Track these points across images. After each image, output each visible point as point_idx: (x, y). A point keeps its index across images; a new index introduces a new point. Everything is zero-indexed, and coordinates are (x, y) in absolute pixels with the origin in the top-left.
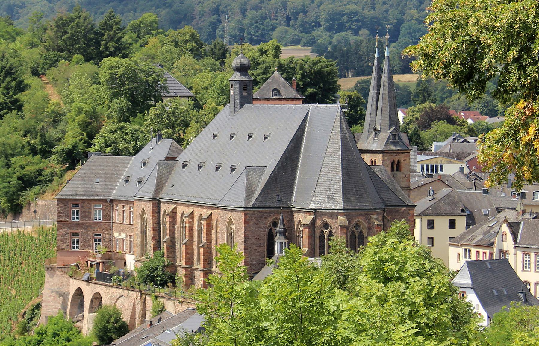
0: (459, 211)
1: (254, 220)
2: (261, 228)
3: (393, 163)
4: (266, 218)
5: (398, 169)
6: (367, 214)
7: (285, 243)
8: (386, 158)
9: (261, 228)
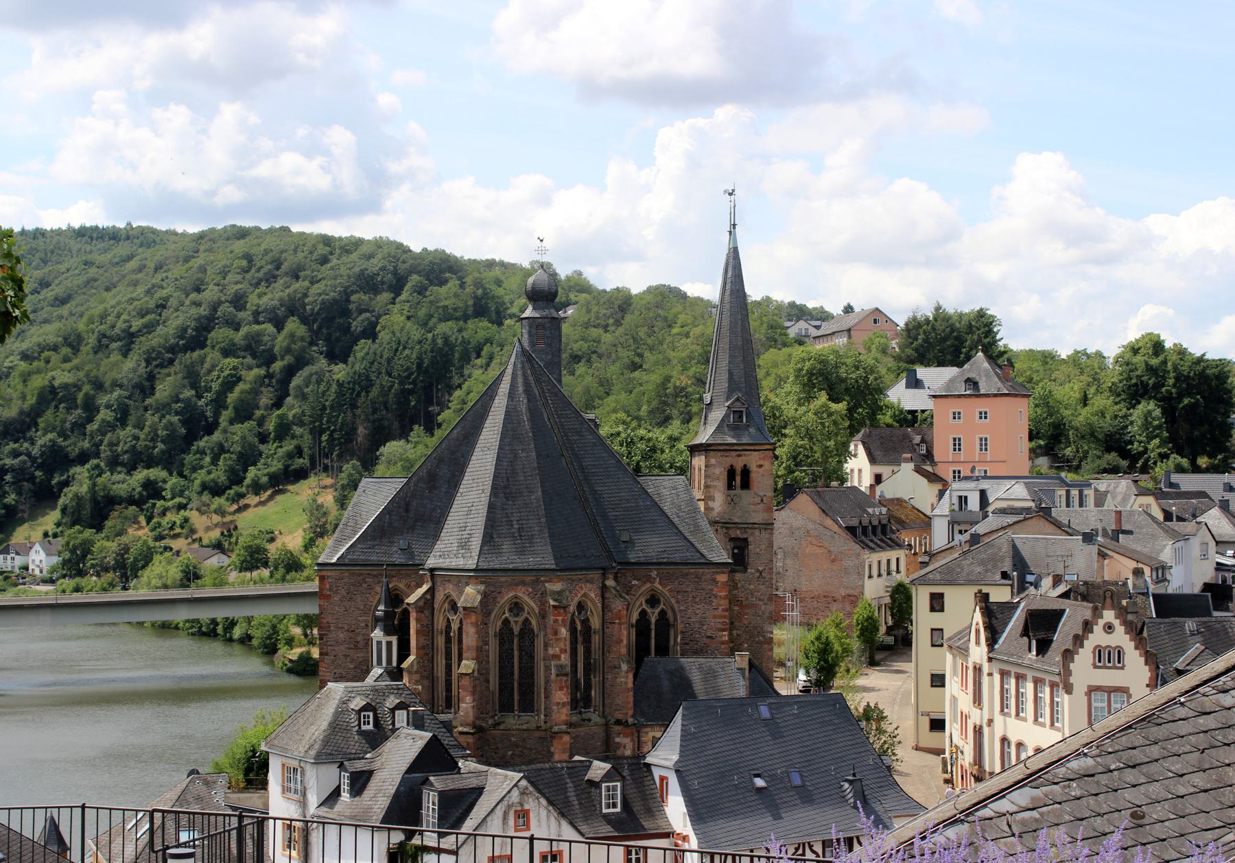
0: (998, 576)
1: (343, 592)
2: (359, 609)
3: (731, 473)
4: (370, 588)
5: (746, 485)
6: (537, 581)
7: (389, 644)
8: (713, 461)
9: (359, 609)
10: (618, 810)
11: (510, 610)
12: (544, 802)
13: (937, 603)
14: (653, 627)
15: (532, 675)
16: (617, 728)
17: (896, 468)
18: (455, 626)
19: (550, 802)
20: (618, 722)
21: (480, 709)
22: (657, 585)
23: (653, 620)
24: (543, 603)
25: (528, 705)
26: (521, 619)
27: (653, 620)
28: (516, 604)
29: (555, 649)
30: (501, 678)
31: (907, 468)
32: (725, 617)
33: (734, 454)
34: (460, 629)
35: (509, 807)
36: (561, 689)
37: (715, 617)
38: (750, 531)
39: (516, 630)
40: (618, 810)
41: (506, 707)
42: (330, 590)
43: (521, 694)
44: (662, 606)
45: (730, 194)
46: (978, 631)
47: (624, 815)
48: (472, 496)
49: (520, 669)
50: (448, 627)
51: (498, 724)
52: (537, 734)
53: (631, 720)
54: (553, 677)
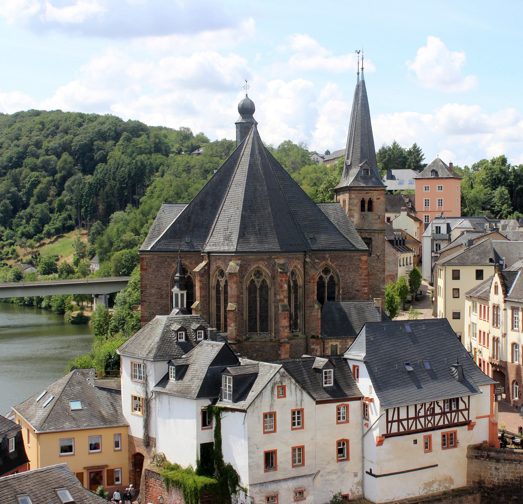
0: (488, 261)
1: (154, 266)
2: (163, 276)
3: (363, 202)
4: (169, 264)
5: (370, 209)
6: (270, 258)
7: (182, 295)
8: (353, 196)
9: (163, 276)
10: (332, 385)
11: (255, 275)
12: (293, 381)
13: (456, 276)
14: (326, 285)
15: (267, 311)
16: (314, 340)
17: (397, 215)
18: (222, 284)
19: (297, 381)
20: (313, 337)
21: (239, 330)
22: (329, 262)
23: (326, 282)
24: (273, 271)
25: (265, 328)
26: (261, 280)
27: (326, 282)
28: (258, 271)
29: (280, 296)
30: (249, 312)
31: (404, 214)
32: (366, 279)
33: (365, 192)
34: (226, 286)
35: (275, 384)
36: (285, 318)
37: (360, 279)
38: (373, 234)
39: (258, 285)
40: (332, 385)
41: (252, 329)
42: (146, 266)
43: (262, 322)
44: (331, 274)
45: (358, 53)
46: (496, 287)
47: (335, 388)
48: (231, 211)
49: (260, 308)
50: (218, 285)
51: (249, 339)
52: (270, 344)
53: (320, 336)
54: (280, 311)
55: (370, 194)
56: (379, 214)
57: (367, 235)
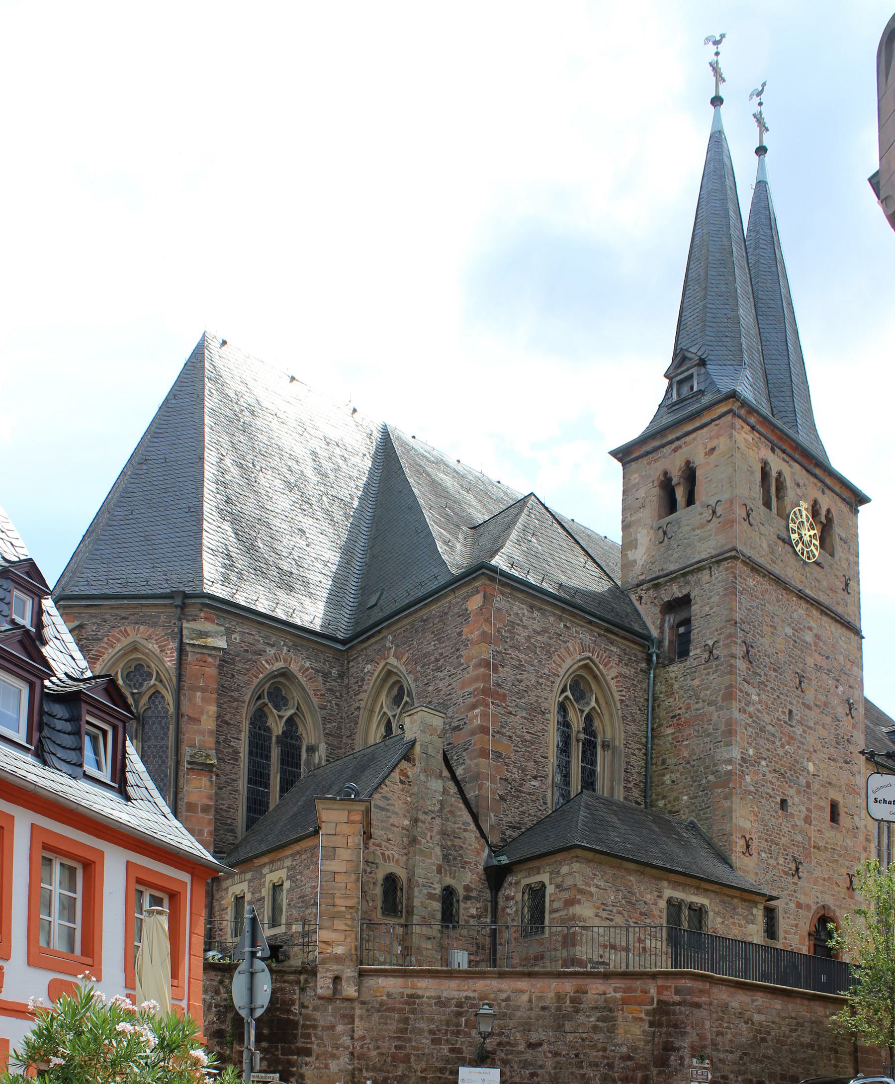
3: (667, 486)
33: (667, 450)
55: (684, 449)
56: (712, 502)
57: (675, 587)
